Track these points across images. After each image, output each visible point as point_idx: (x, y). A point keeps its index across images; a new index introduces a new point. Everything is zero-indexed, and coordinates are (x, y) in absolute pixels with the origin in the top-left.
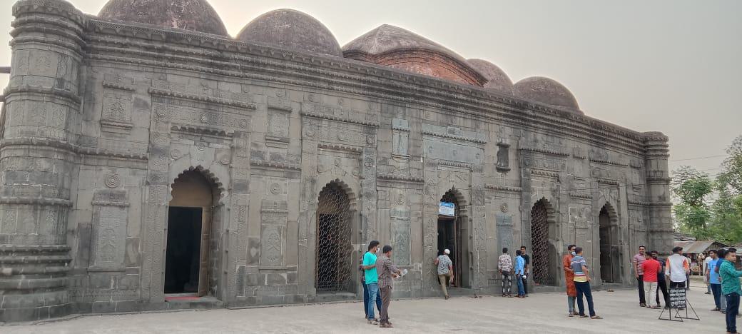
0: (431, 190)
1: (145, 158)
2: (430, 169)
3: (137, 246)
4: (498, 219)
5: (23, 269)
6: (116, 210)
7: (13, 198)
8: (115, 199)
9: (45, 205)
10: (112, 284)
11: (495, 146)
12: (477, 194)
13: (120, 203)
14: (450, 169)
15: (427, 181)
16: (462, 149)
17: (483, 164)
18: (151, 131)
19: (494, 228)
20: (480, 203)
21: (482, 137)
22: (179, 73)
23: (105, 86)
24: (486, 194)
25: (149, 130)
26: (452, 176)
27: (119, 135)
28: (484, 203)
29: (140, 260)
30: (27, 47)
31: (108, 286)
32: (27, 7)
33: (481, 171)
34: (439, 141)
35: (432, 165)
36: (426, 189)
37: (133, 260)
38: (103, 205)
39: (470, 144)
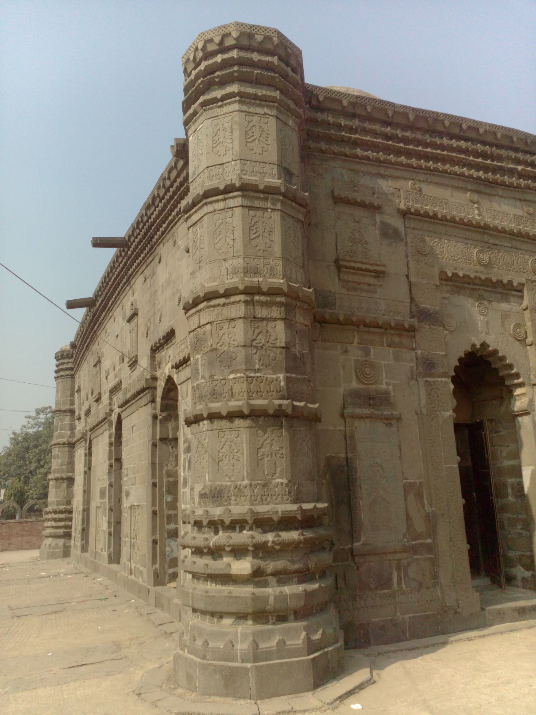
1: (412, 330)
3: (419, 496)
5: (271, 566)
6: (380, 427)
7: (235, 404)
8: (373, 402)
10: (395, 580)
13: (387, 412)
18: (413, 279)
22: (436, 179)
23: (338, 200)
25: (407, 276)
27: (365, 287)
29: (431, 521)
30: (225, 109)
31: (387, 583)
32: (217, 40)
37: (420, 526)
38: (360, 417)
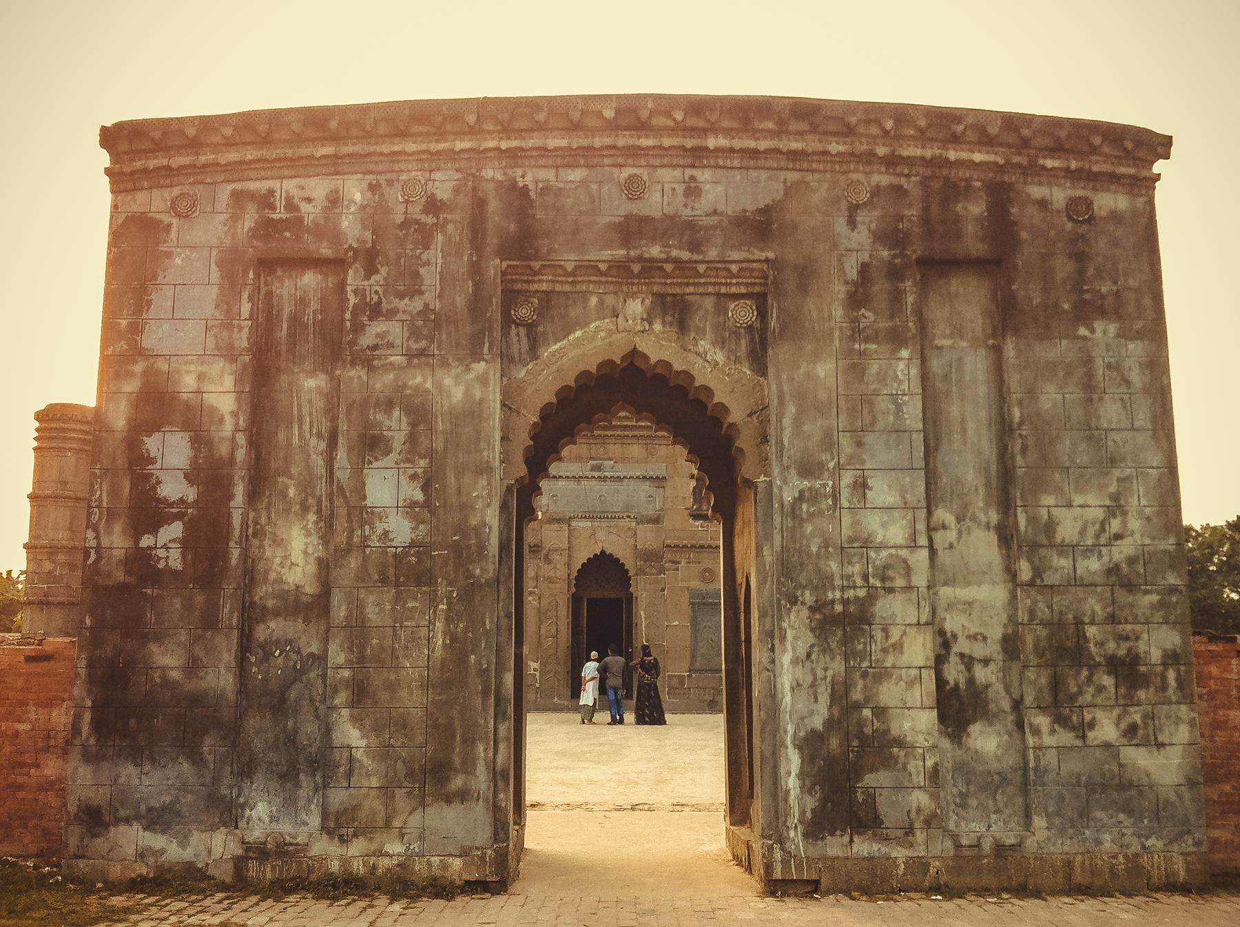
0: (556, 557)
2: (555, 526)
4: (694, 594)
9: (49, 604)
11: (686, 479)
12: (651, 557)
14: (596, 524)
15: (548, 545)
16: (618, 491)
17: (662, 509)
19: (686, 609)
20: (654, 571)
21: (658, 469)
24: (668, 556)
26: (601, 535)
28: (662, 570)
33: (656, 520)
34: (572, 485)
35: (559, 521)
36: (546, 556)
39: (632, 482)
